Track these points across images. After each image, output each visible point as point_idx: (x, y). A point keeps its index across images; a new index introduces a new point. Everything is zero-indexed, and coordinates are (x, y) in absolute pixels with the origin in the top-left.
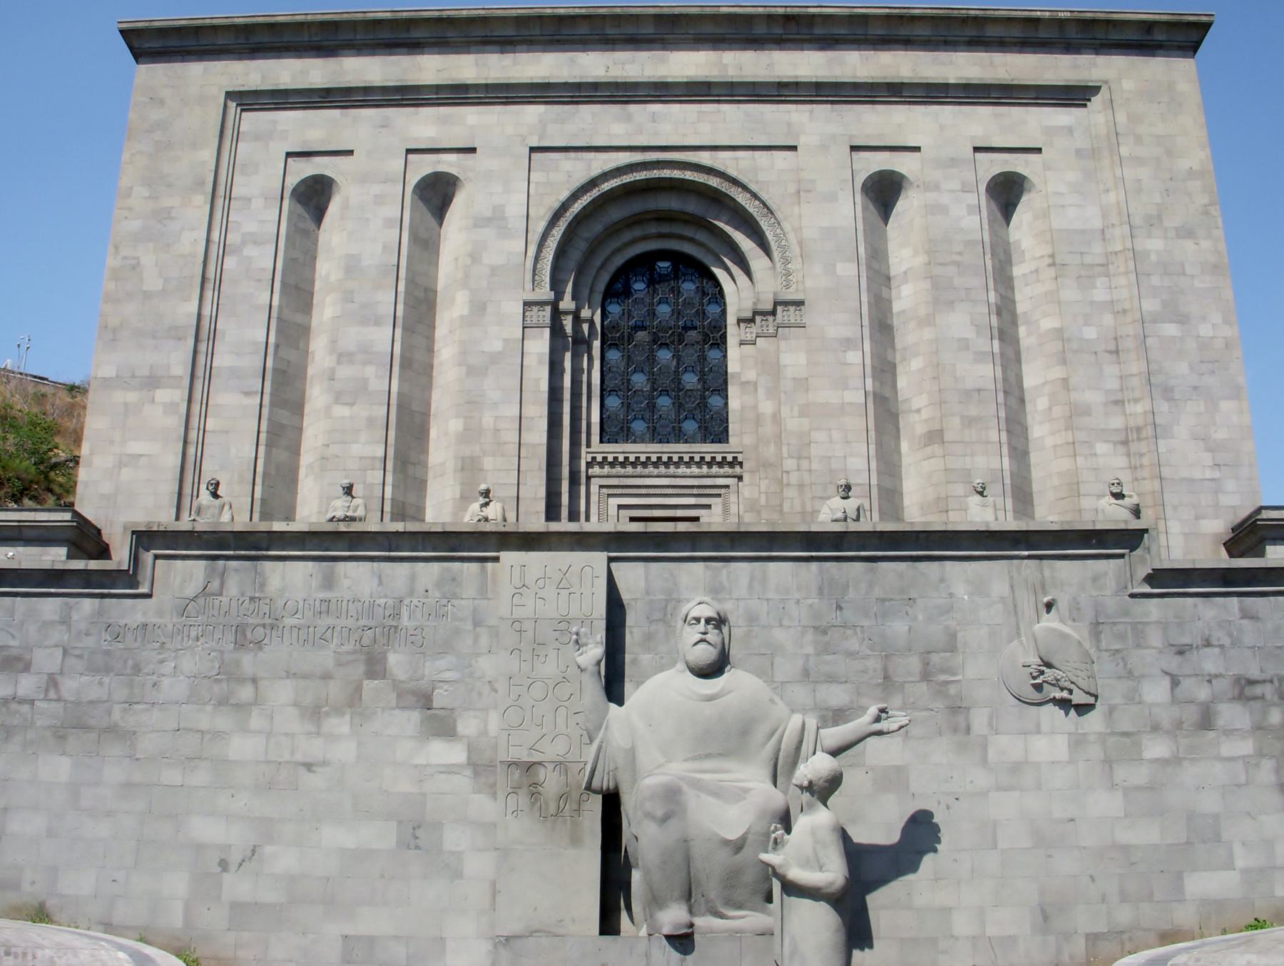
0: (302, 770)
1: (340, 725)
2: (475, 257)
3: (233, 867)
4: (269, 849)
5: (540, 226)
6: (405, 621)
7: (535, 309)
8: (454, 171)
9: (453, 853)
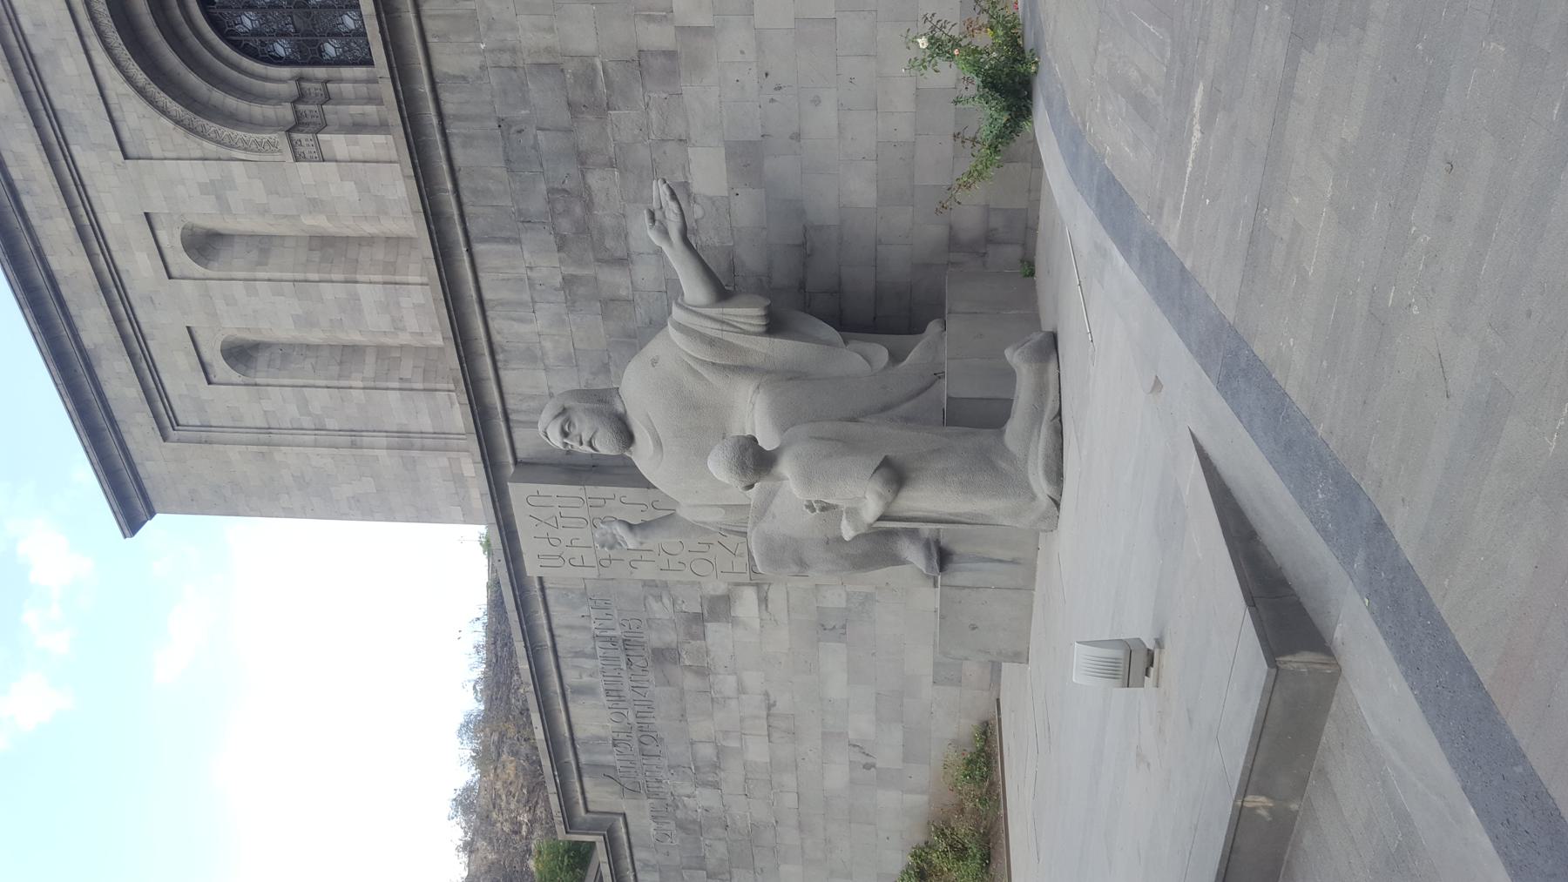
0: (774, 710)
1: (727, 684)
2: (264, 211)
3: (870, 760)
4: (852, 735)
5: (211, 148)
6: (618, 633)
7: (300, 149)
8: (178, 234)
9: (848, 600)
